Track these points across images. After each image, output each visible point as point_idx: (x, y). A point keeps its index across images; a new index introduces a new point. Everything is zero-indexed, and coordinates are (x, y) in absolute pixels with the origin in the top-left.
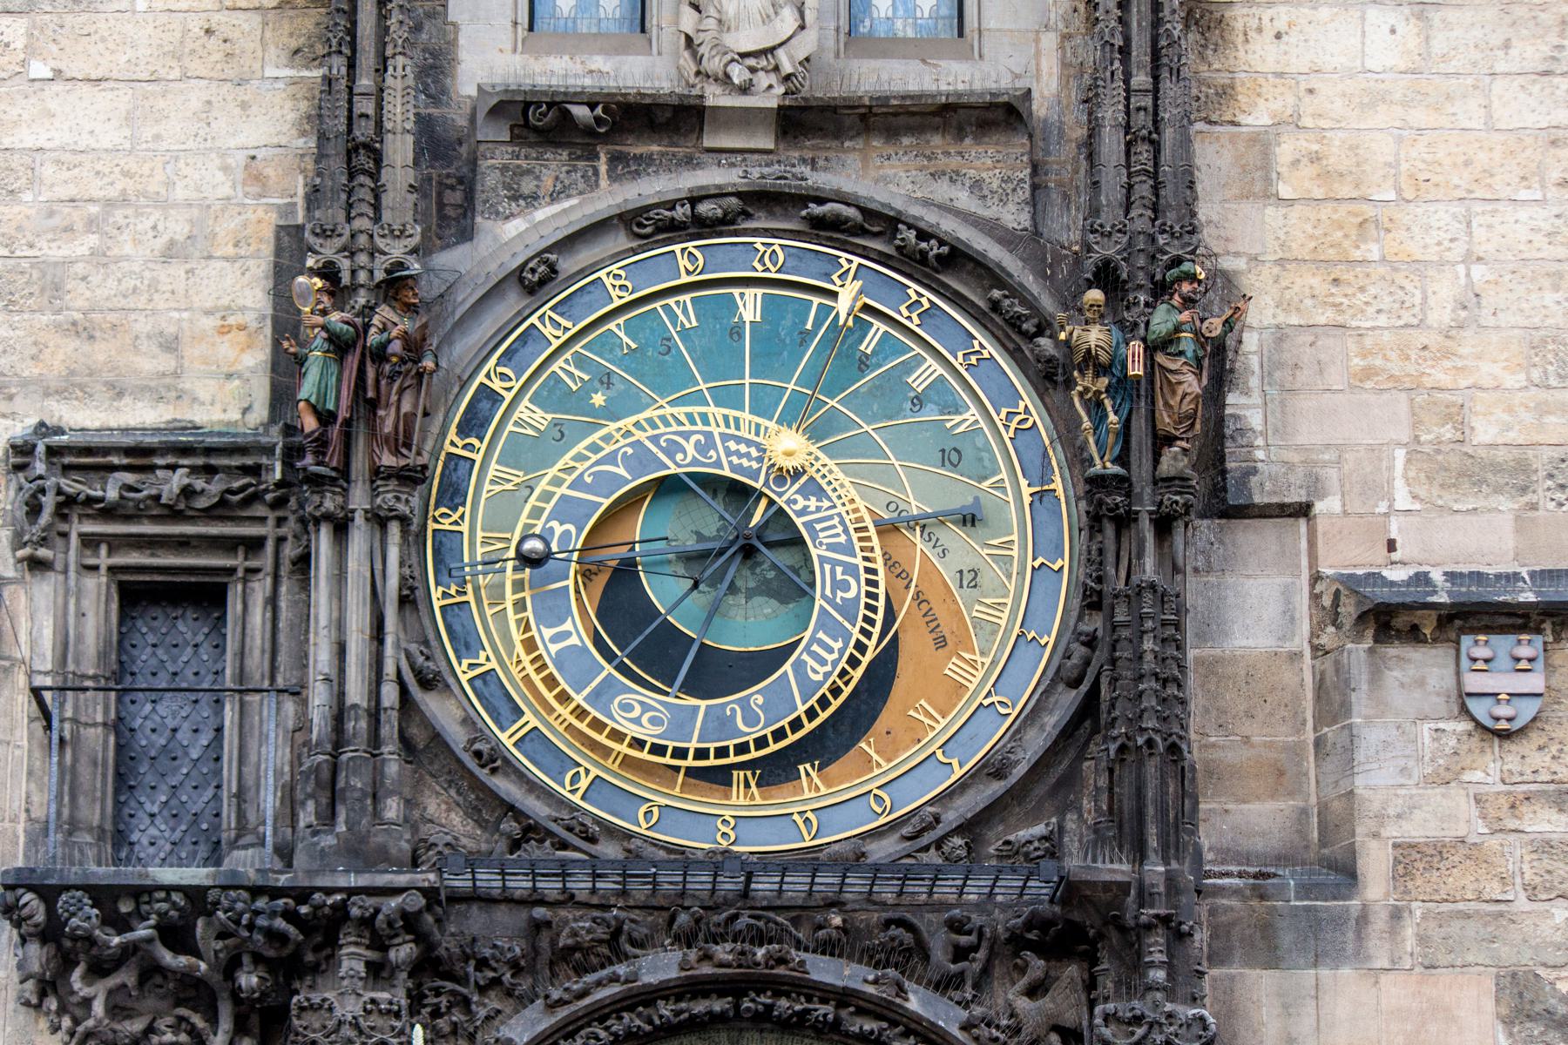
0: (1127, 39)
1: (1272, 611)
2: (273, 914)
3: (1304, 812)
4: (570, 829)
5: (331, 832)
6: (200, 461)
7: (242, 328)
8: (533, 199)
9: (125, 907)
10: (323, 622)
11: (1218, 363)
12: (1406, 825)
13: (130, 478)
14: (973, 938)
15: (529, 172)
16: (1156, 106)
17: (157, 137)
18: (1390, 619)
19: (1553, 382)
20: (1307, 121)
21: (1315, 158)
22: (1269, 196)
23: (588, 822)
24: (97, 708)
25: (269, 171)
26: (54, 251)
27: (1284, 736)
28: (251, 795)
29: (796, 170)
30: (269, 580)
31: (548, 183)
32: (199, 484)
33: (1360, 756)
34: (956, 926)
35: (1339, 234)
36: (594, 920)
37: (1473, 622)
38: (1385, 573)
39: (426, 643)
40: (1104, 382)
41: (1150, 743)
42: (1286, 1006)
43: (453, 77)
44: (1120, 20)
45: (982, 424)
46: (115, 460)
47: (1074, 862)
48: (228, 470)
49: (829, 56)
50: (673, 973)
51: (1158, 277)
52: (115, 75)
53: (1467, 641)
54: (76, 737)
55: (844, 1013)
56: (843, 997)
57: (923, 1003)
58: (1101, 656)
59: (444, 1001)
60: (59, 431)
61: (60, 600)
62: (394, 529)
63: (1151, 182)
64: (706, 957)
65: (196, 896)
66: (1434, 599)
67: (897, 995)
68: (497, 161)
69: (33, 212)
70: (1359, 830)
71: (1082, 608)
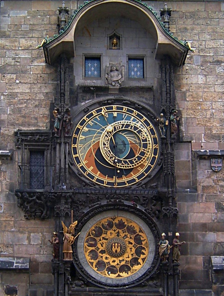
0: (166, 79)
1: (186, 155)
4: (92, 184)
6: (40, 135)
7: (46, 116)
8: (86, 100)
10: (58, 156)
11: (179, 123)
12: (204, 184)
13: (30, 137)
14: (146, 198)
15: (85, 96)
16: (170, 89)
17: (34, 91)
18: (202, 157)
20: (190, 90)
21: (192, 95)
22: (186, 100)
23: (94, 183)
25: (50, 96)
27: (188, 172)
28: (48, 179)
29: (121, 96)
30: (50, 151)
31: (88, 98)
32: (40, 138)
33: (198, 174)
34: (144, 197)
35: (195, 105)
36: (95, 196)
39: (72, 159)
40: (163, 125)
44: (165, 77)
46: (29, 134)
47: (159, 189)
48: (44, 136)
49: (126, 81)
50: (106, 203)
51: (170, 111)
52: (28, 82)
53: (212, 159)
57: (140, 207)
58: (163, 161)
59: (75, 206)
60: (21, 130)
62: (67, 144)
64: (110, 201)
66: (207, 154)
70: (197, 184)
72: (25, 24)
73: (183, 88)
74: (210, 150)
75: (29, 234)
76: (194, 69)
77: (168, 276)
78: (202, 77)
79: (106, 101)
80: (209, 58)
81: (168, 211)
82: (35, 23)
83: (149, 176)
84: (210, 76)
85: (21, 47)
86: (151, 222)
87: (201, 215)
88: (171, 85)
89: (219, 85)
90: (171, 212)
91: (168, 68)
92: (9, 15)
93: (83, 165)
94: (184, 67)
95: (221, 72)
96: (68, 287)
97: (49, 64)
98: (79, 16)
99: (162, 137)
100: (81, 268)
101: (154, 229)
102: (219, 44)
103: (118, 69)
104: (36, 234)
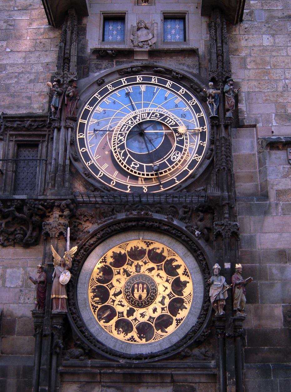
1: (249, 146)
3: (257, 185)
4: (104, 189)
5: (54, 189)
6: (34, 119)
7: (43, 95)
8: (101, 69)
9: (9, 204)
11: (236, 97)
15: (100, 64)
17: (30, 61)
18: (273, 145)
20: (252, 55)
21: (254, 61)
22: (246, 68)
23: (108, 187)
30: (46, 142)
31: (104, 66)
33: (268, 173)
34: (185, 207)
38: (272, 137)
39: (76, 153)
40: (213, 100)
41: (224, 168)
43: (87, 49)
44: (215, 34)
45: (189, 110)
46: (16, 119)
48: (38, 121)
50: (124, 217)
54: (6, 173)
55: (160, 225)
56: (160, 221)
57: (178, 223)
60: (7, 114)
61: (5, 146)
62: (70, 130)
63: (222, 63)
64: (131, 213)
65: (23, 200)
67: (172, 221)
69: (5, 75)
70: (268, 187)
71: (210, 144)
73: (242, 52)
74: (284, 136)
75: (4, 271)
76: (256, 27)
77: (224, 339)
78: (268, 36)
80: (276, 12)
81: (223, 227)
83: (192, 176)
84: (279, 36)
85: (17, 7)
86: (196, 246)
88: (224, 43)
91: (219, 22)
94: (242, 24)
96: (57, 359)
97: (53, 25)
99: (212, 115)
100: (83, 328)
103: (147, 25)
104: (15, 269)
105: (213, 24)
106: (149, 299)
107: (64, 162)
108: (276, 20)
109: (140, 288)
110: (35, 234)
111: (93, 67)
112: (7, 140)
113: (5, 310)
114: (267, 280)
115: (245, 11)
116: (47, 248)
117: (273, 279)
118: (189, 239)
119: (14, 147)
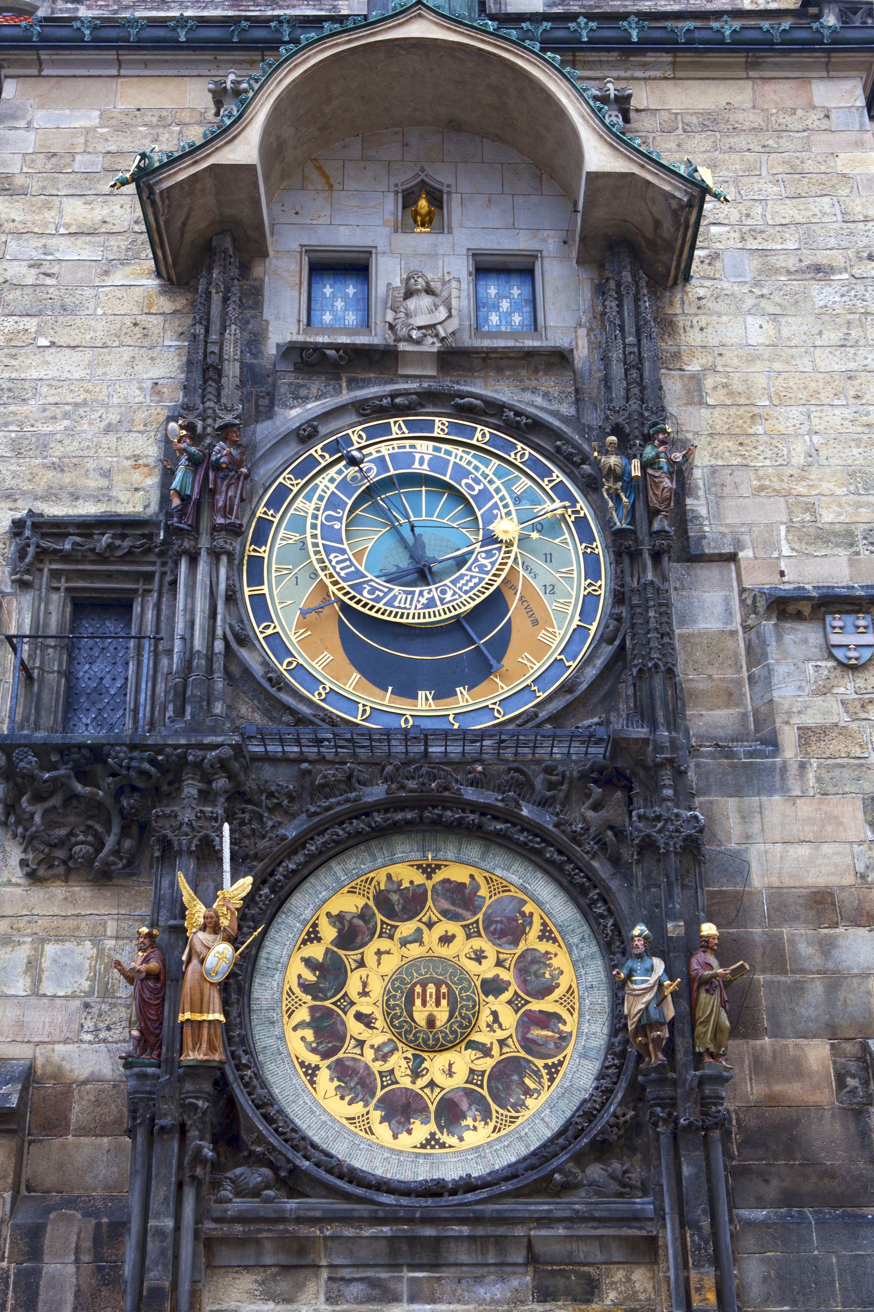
0: (622, 319)
1: (719, 609)
2: (142, 760)
3: (745, 715)
4: (323, 720)
6: (119, 531)
8: (306, 399)
9: (54, 758)
10: (181, 608)
15: (303, 386)
17: (105, 374)
18: (786, 607)
19: (862, 491)
20: (719, 368)
21: (725, 386)
22: (702, 403)
24: (55, 660)
25: (165, 390)
26: (45, 429)
27: (730, 674)
30: (156, 594)
31: (314, 390)
32: (118, 542)
33: (775, 680)
34: (549, 770)
36: (337, 769)
37: (832, 609)
39: (242, 621)
41: (656, 666)
42: (743, 818)
44: (618, 312)
52: (84, 344)
53: (828, 618)
55: (484, 819)
56: (483, 810)
57: (529, 811)
58: (626, 624)
59: (247, 816)
61: (36, 604)
62: (224, 559)
64: (403, 787)
68: (285, 383)
70: (777, 720)
71: (614, 603)
72: (89, 153)
75: (36, 949)
77: (675, 1138)
78: (760, 321)
79: (385, 396)
81: (660, 825)
82: (125, 150)
84: (791, 320)
85: (67, 226)
87: (804, 851)
89: (829, 349)
90: (671, 828)
91: (630, 279)
92: (29, 123)
93: (278, 629)
94: (689, 288)
95: (834, 303)
96: (199, 1199)
97: (169, 279)
98: (281, 81)
100: (267, 1107)
101: (598, 911)
102: (817, 212)
103: (436, 285)
104: (68, 945)
105: (612, 284)
106: (455, 1027)
107: (210, 646)
108: (783, 278)
109: (431, 995)
110: (127, 844)
111: (285, 394)
112: (44, 587)
113: (40, 1062)
114: (784, 972)
115: (697, 253)
116: (165, 883)
117: (803, 971)
118: (565, 858)
119: (64, 607)
